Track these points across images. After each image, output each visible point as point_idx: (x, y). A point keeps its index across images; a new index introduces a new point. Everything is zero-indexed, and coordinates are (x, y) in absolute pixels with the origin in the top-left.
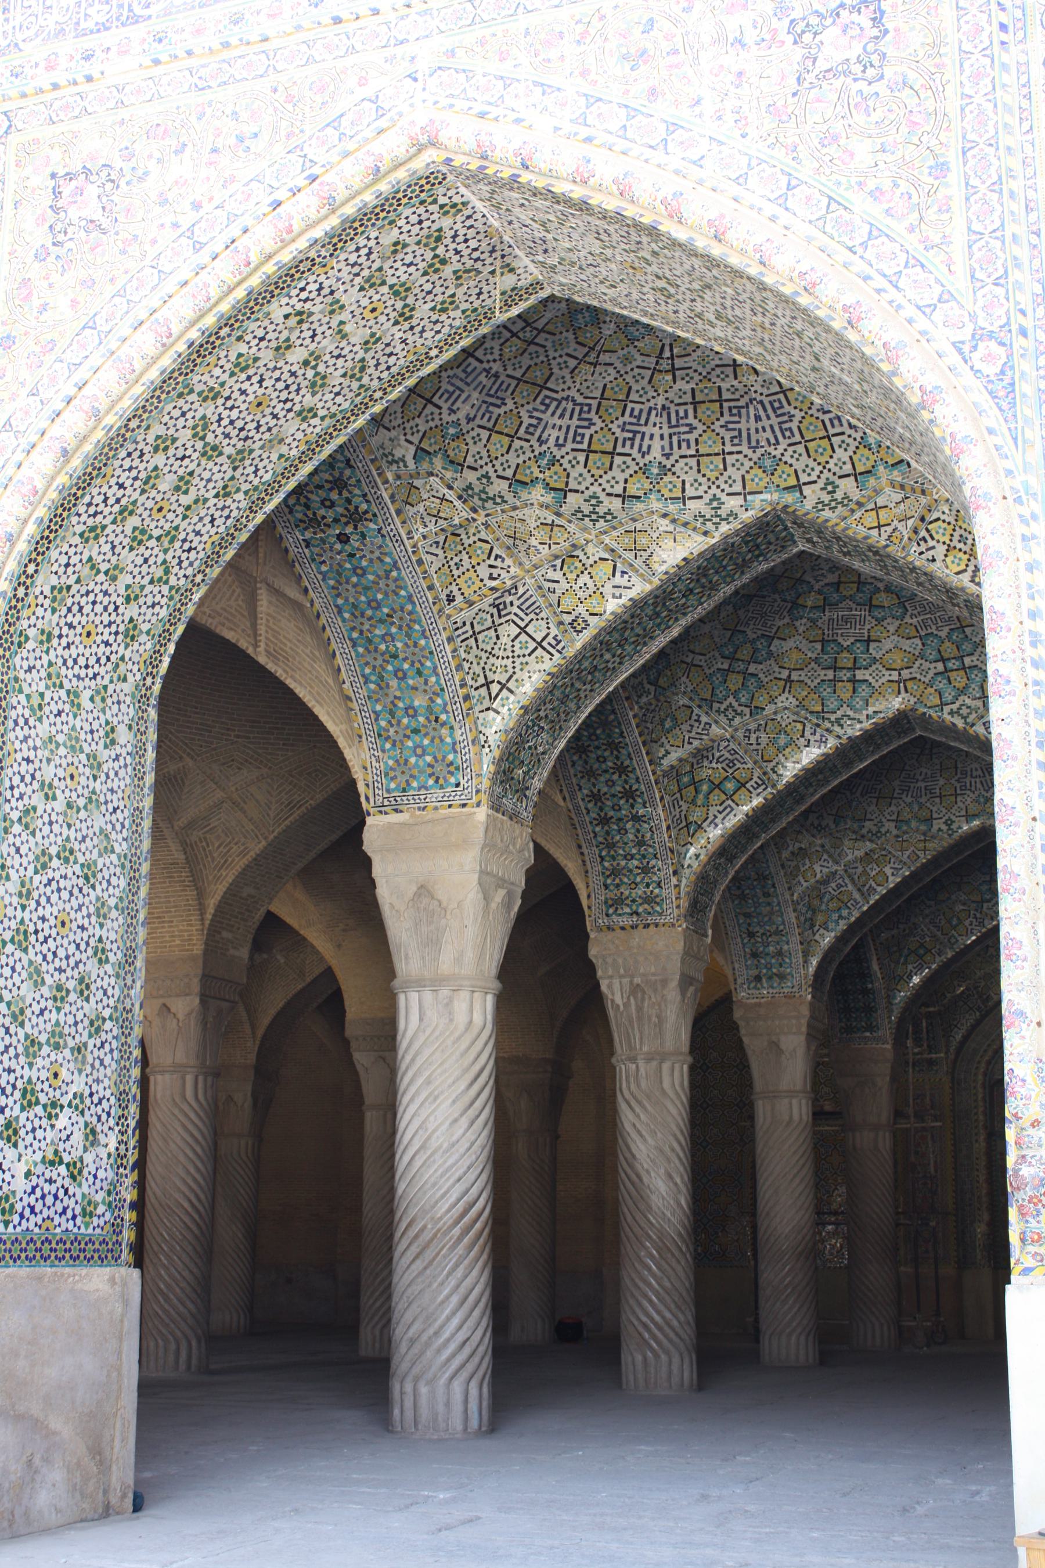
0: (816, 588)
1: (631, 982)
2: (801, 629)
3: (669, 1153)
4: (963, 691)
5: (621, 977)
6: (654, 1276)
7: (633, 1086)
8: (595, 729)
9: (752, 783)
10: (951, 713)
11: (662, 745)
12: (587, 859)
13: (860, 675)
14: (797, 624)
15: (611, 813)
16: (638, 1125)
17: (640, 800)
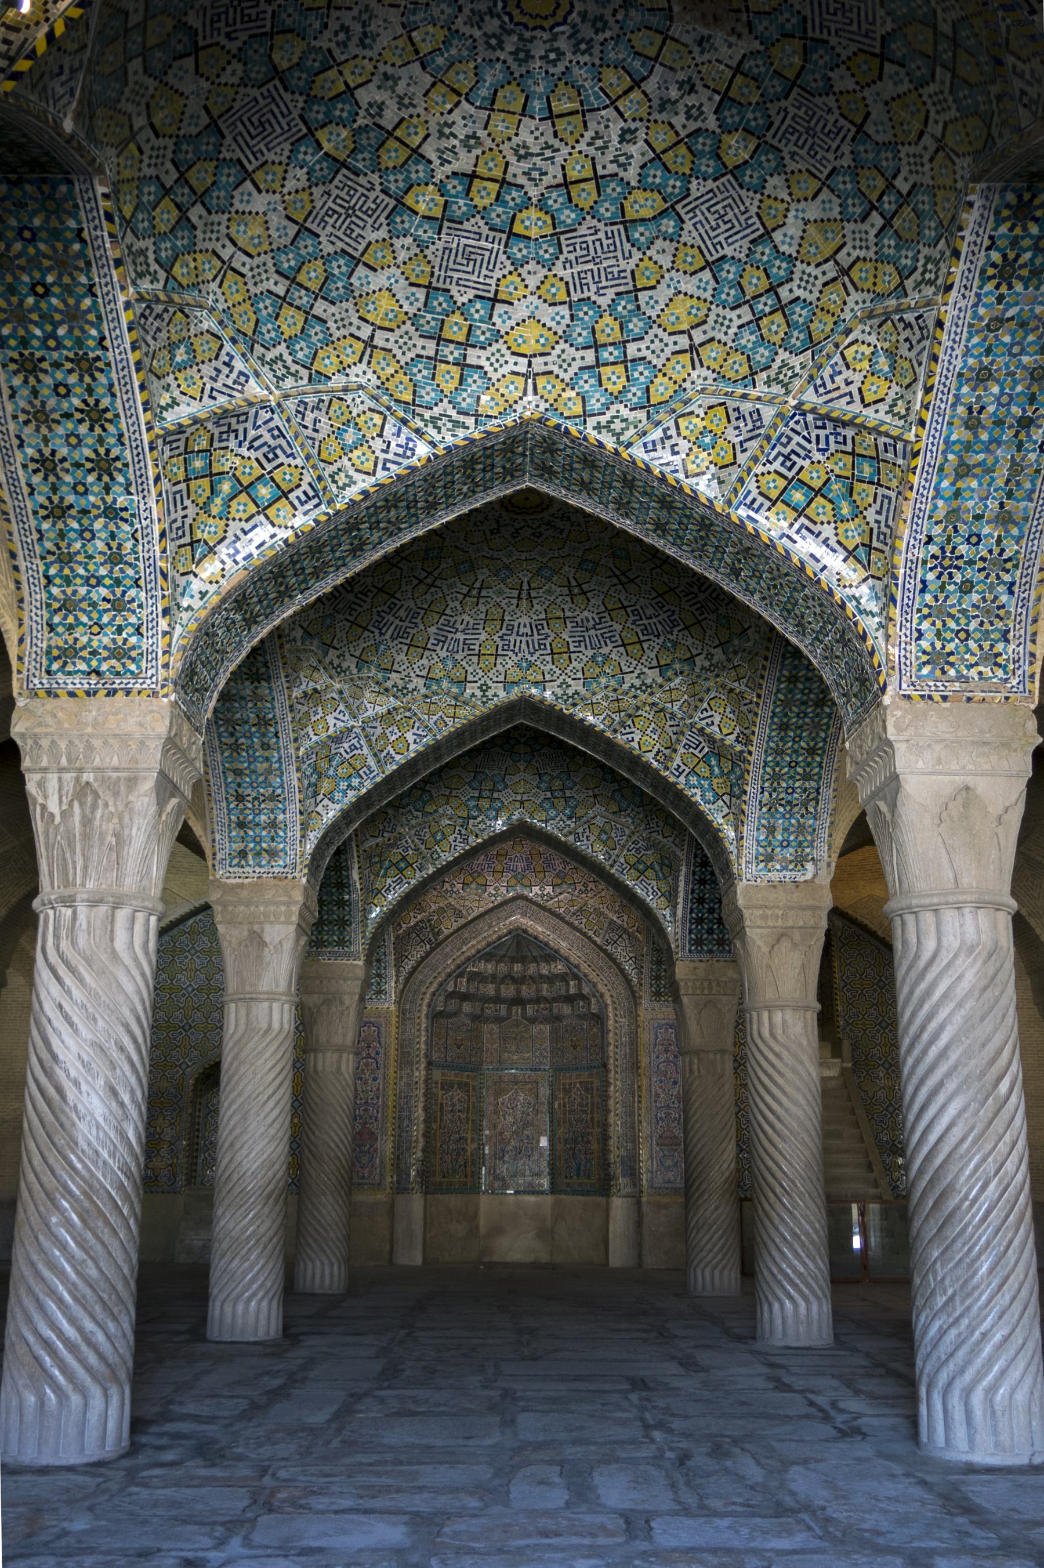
0: (439, 176)
1: (77, 779)
2: (402, 256)
3: (115, 1054)
4: (617, 397)
5: (61, 770)
6: (71, 1258)
7: (64, 944)
8: (56, 325)
9: (299, 492)
10: (598, 427)
11: (167, 388)
12: (23, 578)
13: (474, 356)
14: (398, 243)
15: (71, 499)
16: (67, 1007)
17: (121, 479)
